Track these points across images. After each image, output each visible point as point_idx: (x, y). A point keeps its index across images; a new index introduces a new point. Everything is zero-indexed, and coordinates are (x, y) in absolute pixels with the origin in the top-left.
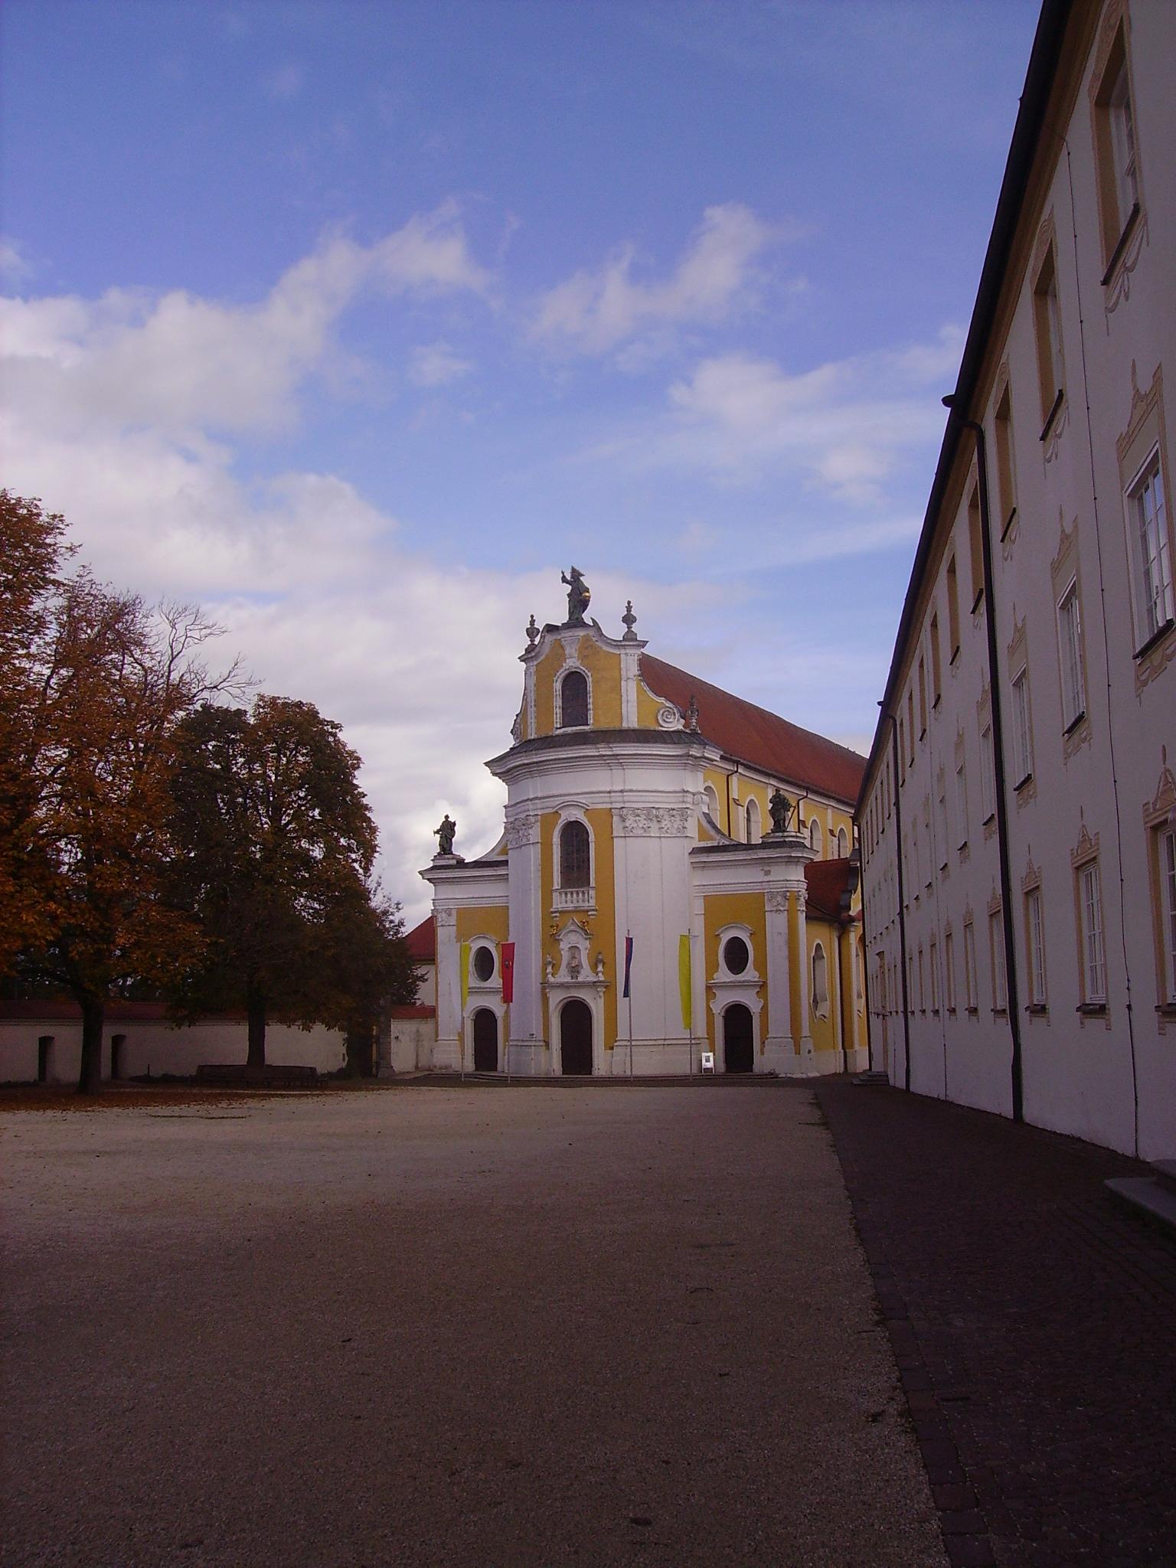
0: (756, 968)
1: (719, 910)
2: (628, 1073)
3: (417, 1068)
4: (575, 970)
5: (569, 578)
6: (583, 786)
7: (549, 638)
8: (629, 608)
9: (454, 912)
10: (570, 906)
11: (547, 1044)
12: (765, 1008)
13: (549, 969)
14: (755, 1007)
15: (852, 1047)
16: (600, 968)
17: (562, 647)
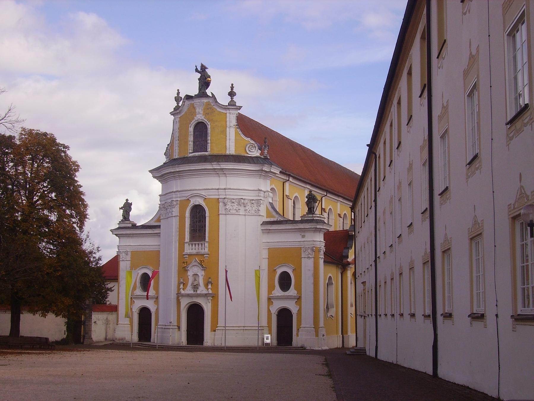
0: (296, 288)
1: (276, 256)
2: (223, 345)
3: (106, 339)
4: (195, 287)
5: (199, 69)
6: (204, 185)
7: (187, 103)
8: (232, 88)
9: (129, 253)
10: (194, 252)
11: (179, 328)
12: (300, 311)
13: (182, 286)
14: (294, 310)
15: (347, 333)
16: (210, 286)
17: (194, 108)
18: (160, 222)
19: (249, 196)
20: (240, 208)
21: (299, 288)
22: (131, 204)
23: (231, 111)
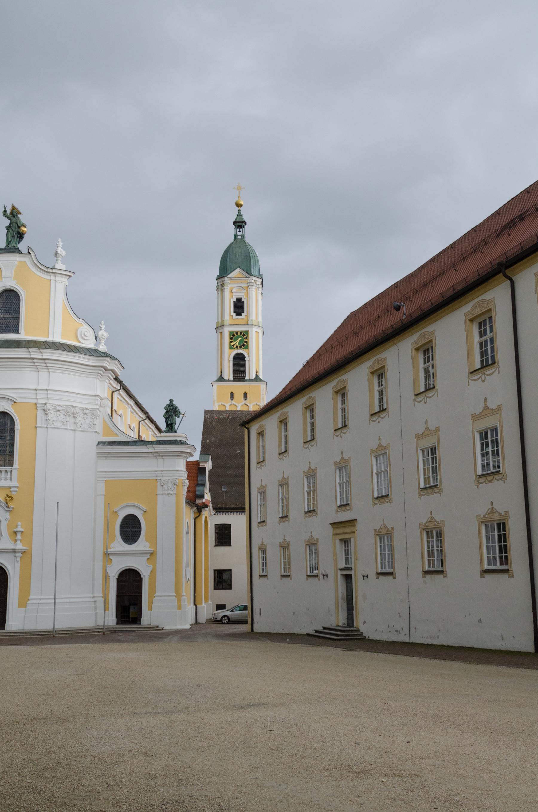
5: (9, 212)
12: (153, 573)
15: (201, 604)
19: (80, 404)
21: (153, 539)
23: (57, 278)
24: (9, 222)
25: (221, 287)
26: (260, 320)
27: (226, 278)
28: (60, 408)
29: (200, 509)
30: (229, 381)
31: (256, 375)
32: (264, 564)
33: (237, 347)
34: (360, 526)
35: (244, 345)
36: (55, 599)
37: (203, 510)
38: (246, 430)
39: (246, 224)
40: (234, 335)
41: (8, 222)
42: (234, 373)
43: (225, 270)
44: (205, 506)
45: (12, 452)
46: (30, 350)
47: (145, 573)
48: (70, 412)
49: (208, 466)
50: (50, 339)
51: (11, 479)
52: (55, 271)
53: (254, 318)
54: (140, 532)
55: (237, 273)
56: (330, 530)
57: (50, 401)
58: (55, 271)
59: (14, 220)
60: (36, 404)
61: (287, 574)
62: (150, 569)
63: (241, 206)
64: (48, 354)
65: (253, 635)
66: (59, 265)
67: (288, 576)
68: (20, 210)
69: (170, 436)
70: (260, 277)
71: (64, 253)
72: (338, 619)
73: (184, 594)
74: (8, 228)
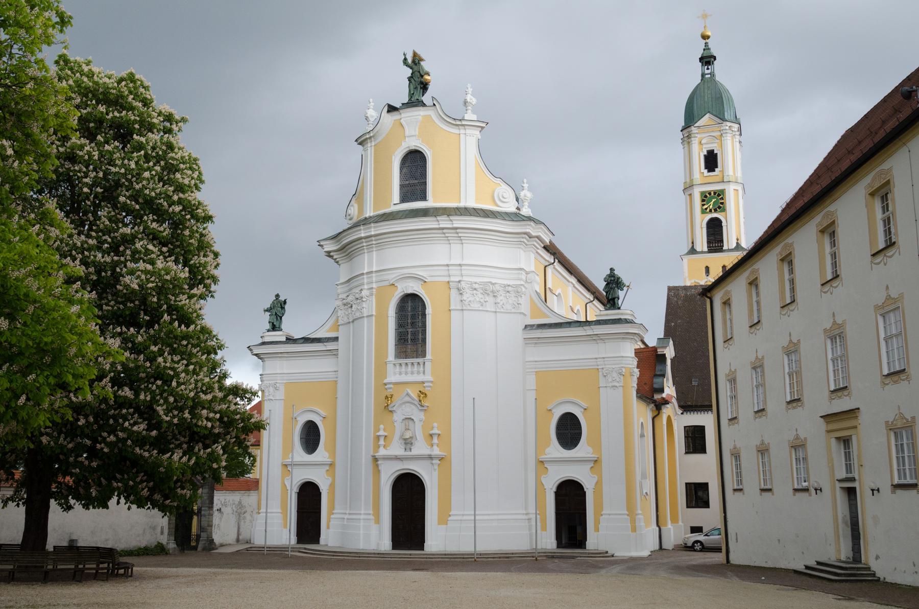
3: (238, 540)
4: (408, 443)
9: (282, 388)
12: (599, 484)
15: (666, 525)
18: (338, 331)
19: (501, 279)
20: (487, 298)
21: (596, 444)
22: (285, 302)
24: (411, 71)
25: (687, 139)
26: (739, 174)
27: (693, 128)
28: (476, 286)
29: (659, 406)
30: (702, 252)
31: (737, 243)
32: (739, 474)
33: (711, 211)
34: (864, 418)
35: (719, 207)
36: (475, 515)
37: (663, 407)
38: (708, 301)
39: (715, 59)
40: (706, 196)
41: (409, 72)
42: (709, 242)
43: (691, 118)
44: (666, 402)
45: (424, 340)
46: (439, 218)
47: (589, 486)
48: (489, 290)
49: (670, 352)
50: (462, 204)
51: (424, 373)
52: (464, 123)
53: (731, 173)
54: (580, 434)
55: (706, 119)
56: (822, 425)
57: (465, 278)
58: (464, 123)
59: (416, 68)
60: (448, 282)
61: (768, 487)
62: (595, 480)
63: (708, 37)
64: (459, 222)
65: (728, 568)
66: (470, 116)
67: (770, 490)
68: (423, 56)
69: (612, 314)
70: (737, 121)
71: (474, 101)
72: (837, 551)
73: (640, 512)
74: (410, 79)
